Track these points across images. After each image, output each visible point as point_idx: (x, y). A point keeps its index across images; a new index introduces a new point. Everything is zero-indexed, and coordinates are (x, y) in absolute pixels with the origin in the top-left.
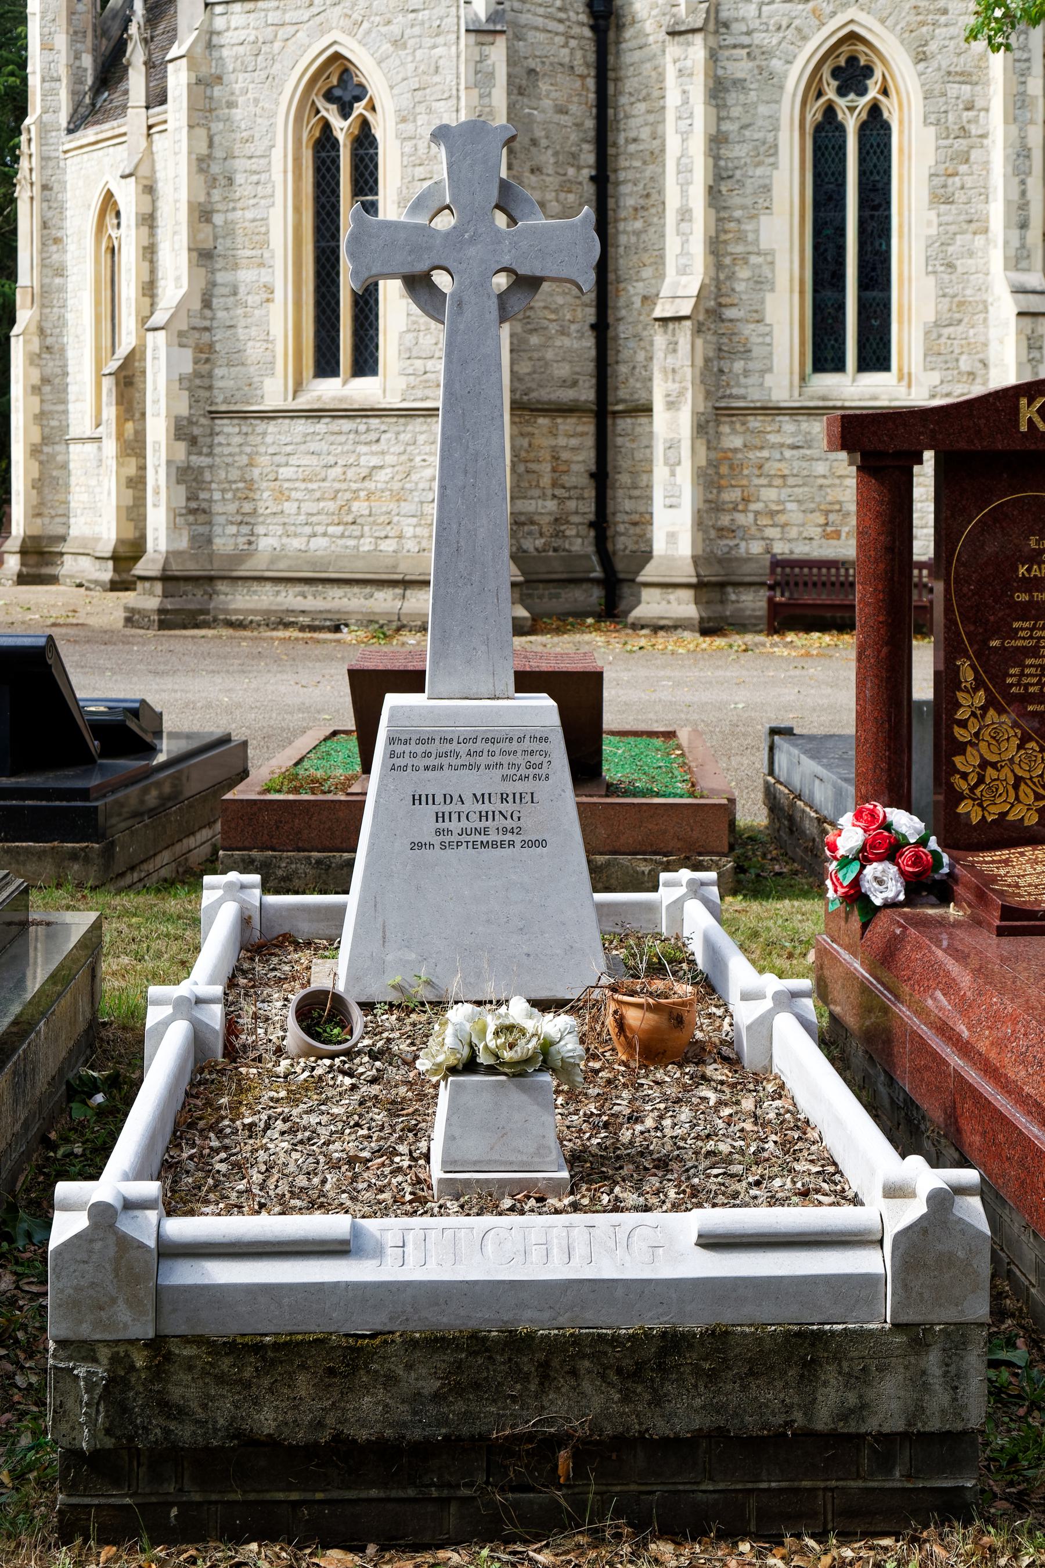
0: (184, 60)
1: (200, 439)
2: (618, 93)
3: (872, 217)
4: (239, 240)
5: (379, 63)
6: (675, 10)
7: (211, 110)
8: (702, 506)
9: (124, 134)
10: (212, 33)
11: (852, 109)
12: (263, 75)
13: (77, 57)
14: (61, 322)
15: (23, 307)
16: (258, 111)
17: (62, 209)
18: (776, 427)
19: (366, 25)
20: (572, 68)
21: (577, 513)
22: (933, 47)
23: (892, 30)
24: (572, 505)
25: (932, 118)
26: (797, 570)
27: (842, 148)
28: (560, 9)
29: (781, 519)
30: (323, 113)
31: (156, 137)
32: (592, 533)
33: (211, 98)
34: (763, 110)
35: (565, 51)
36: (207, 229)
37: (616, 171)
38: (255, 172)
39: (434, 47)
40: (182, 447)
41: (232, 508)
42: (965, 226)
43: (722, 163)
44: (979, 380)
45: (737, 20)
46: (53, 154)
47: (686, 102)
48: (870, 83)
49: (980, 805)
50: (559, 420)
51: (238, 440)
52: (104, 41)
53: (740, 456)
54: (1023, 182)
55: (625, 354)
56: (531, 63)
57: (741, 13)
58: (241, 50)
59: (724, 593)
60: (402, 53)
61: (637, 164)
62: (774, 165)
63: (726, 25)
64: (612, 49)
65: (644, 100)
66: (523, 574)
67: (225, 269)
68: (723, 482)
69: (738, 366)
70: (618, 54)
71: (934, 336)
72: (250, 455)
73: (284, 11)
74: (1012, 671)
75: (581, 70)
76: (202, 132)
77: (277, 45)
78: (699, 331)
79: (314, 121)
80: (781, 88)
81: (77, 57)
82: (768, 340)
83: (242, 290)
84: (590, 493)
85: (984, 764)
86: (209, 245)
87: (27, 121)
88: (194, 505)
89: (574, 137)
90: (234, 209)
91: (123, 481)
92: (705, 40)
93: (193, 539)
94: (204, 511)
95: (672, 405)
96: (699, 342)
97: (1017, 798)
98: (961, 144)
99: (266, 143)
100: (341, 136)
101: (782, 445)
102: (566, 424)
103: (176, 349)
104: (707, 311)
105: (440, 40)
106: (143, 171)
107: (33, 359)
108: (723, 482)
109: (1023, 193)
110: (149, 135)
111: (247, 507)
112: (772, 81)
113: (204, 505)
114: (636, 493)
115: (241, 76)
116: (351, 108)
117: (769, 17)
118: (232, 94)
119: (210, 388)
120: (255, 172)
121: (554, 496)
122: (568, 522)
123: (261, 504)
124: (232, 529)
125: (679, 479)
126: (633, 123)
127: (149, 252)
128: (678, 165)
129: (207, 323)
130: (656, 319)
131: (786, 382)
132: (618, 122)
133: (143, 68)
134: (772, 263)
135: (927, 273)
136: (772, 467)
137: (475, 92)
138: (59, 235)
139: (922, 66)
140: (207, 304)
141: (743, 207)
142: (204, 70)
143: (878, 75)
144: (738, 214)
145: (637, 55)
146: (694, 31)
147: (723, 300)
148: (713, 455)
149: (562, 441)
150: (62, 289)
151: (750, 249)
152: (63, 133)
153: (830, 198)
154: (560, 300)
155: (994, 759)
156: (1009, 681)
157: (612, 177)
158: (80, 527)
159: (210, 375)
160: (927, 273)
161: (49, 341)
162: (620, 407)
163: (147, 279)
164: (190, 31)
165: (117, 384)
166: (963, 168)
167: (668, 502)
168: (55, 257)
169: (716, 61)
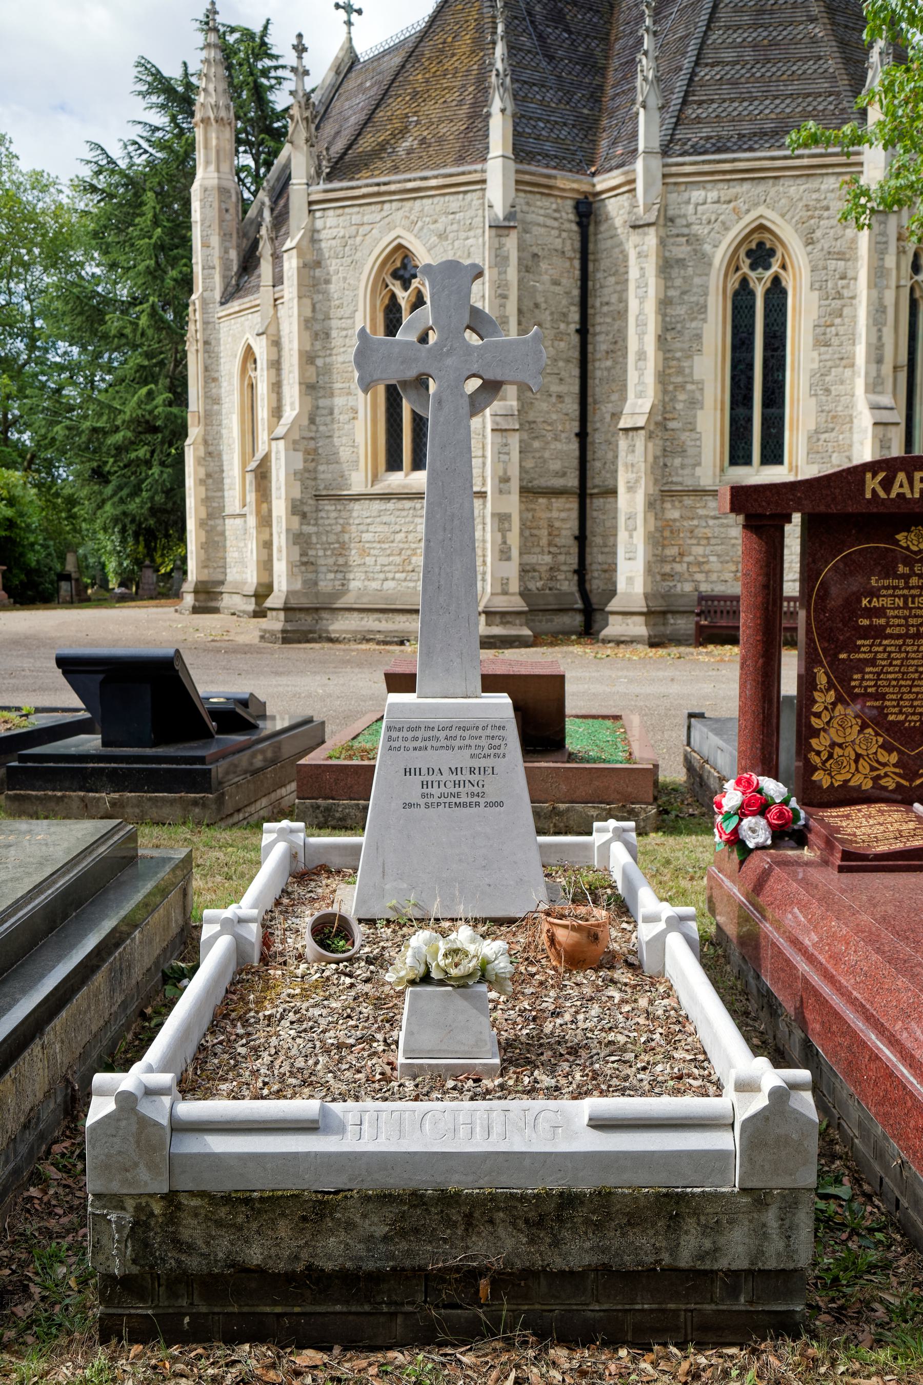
0: (295, 251)
1: (308, 515)
2: (596, 270)
3: (773, 356)
4: (335, 376)
5: (429, 251)
6: (636, 210)
7: (314, 286)
8: (651, 559)
9: (258, 305)
10: (315, 231)
11: (760, 280)
12: (349, 260)
13: (226, 252)
14: (218, 436)
15: (193, 425)
16: (346, 286)
17: (218, 358)
18: (703, 504)
19: (420, 224)
20: (563, 252)
21: (565, 564)
22: (818, 234)
23: (789, 222)
24: (562, 558)
25: (817, 285)
26: (716, 603)
27: (752, 307)
28: (555, 211)
29: (706, 567)
30: (391, 287)
31: (280, 307)
32: (576, 578)
33: (314, 277)
34: (697, 281)
35: (559, 240)
36: (312, 370)
37: (593, 326)
38: (345, 329)
39: (467, 238)
40: (296, 520)
41: (331, 561)
43: (668, 319)
45: (679, 216)
46: (211, 320)
47: (643, 276)
48: (773, 260)
49: (829, 774)
50: (553, 500)
51: (333, 515)
52: (245, 241)
53: (678, 524)
55: (599, 454)
56: (535, 250)
57: (683, 211)
58: (333, 242)
59: (665, 619)
60: (445, 243)
61: (608, 320)
62: (704, 320)
63: (672, 220)
64: (592, 239)
65: (614, 275)
66: (528, 605)
67: (324, 397)
68: (666, 542)
69: (677, 461)
70: (596, 242)
72: (343, 526)
73: (363, 215)
74: (855, 677)
75: (570, 254)
76: (307, 302)
77: (359, 239)
78: (650, 437)
79: (384, 292)
80: (710, 265)
81: (226, 252)
82: (698, 443)
83: (336, 411)
84: (575, 550)
85: (833, 745)
86: (314, 380)
87: (193, 297)
88: (305, 559)
89: (564, 302)
90: (330, 355)
91: (261, 543)
92: (657, 231)
93: (305, 582)
94: (312, 564)
95: (631, 489)
96: (650, 445)
97: (857, 769)
99: (352, 308)
100: (403, 303)
101: (707, 516)
102: (558, 503)
103: (292, 452)
104: (657, 424)
105: (471, 233)
106: (272, 330)
107: (199, 461)
108: (666, 542)
110: (275, 306)
111: (341, 561)
112: (704, 260)
113: (312, 559)
114: (606, 550)
115: (334, 261)
116: (410, 283)
117: (703, 214)
118: (328, 274)
119: (315, 479)
120: (345, 329)
121: (550, 552)
122: (559, 570)
123: (351, 558)
124: (331, 576)
125: (635, 541)
126: (606, 291)
127: (277, 387)
128: (637, 320)
129: (312, 434)
130: (621, 429)
131: (710, 473)
132: (595, 290)
133: (270, 259)
134: (702, 389)
135: (811, 396)
136: (700, 532)
137: (496, 270)
138: (216, 375)
139: (810, 247)
140: (312, 421)
141: (682, 350)
142: (309, 258)
143: (779, 254)
144: (678, 354)
145: (609, 243)
146: (649, 225)
147: (667, 416)
148: (659, 523)
149: (555, 514)
150: (219, 413)
151: (687, 379)
152: (218, 305)
153: (743, 343)
154: (554, 417)
155: (840, 741)
156: (853, 683)
157: (591, 330)
158: (232, 575)
159: (315, 470)
160: (811, 396)
161: (211, 449)
162: (595, 491)
163: (275, 405)
164: (299, 230)
165: (256, 478)
167: (628, 556)
168: (214, 391)
169: (664, 246)
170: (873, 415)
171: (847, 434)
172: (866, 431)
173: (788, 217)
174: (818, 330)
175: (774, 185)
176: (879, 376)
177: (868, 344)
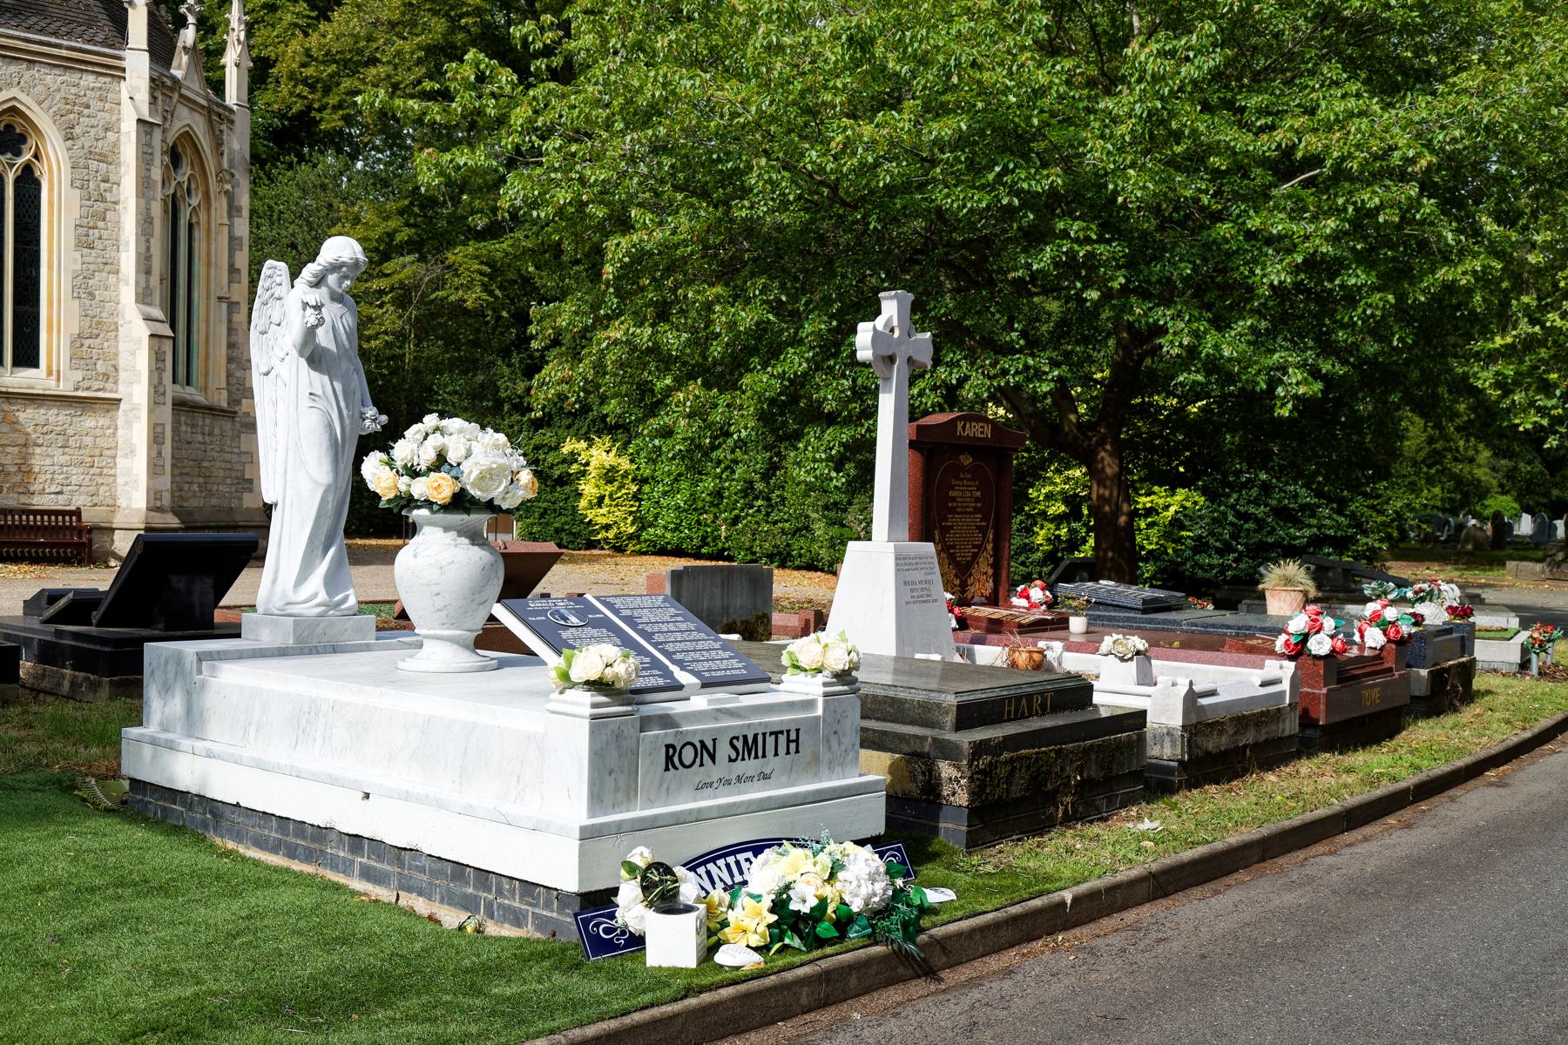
22: (78, 130)
25: (78, 184)
42: (102, 266)
44: (111, 380)
54: (148, 241)
71: (78, 344)
98: (100, 206)
109: (148, 249)
139: (70, 143)
143: (32, 142)
166: (101, 224)
170: (149, 327)
171: (112, 342)
172: (139, 341)
173: (44, 105)
174: (80, 230)
175: (28, 69)
176: (147, 287)
177: (138, 254)
